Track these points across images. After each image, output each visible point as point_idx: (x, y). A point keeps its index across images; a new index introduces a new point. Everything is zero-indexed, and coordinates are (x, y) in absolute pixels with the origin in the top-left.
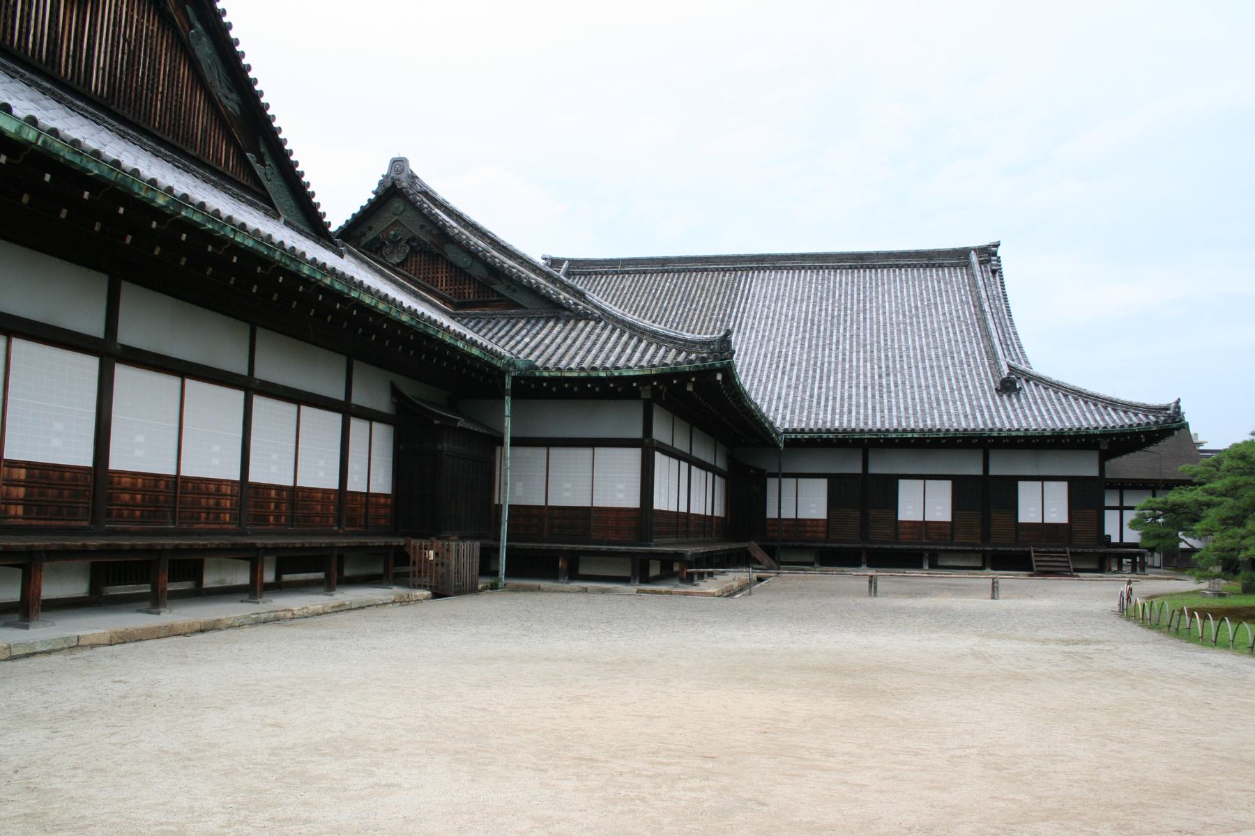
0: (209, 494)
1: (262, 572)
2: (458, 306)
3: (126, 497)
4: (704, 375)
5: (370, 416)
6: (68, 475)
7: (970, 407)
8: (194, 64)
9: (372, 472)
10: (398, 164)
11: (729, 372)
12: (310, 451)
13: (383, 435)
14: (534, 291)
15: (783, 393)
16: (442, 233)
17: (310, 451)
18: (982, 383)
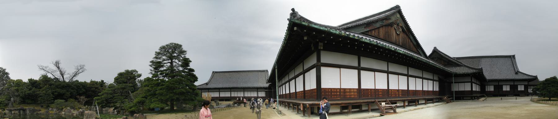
2: (445, 65)
4: (479, 73)
5: (436, 81)
7: (511, 76)
9: (437, 89)
10: (435, 48)
11: (482, 72)
12: (429, 86)
13: (437, 83)
14: (455, 63)
15: (488, 75)
16: (442, 56)
17: (429, 86)
18: (513, 72)
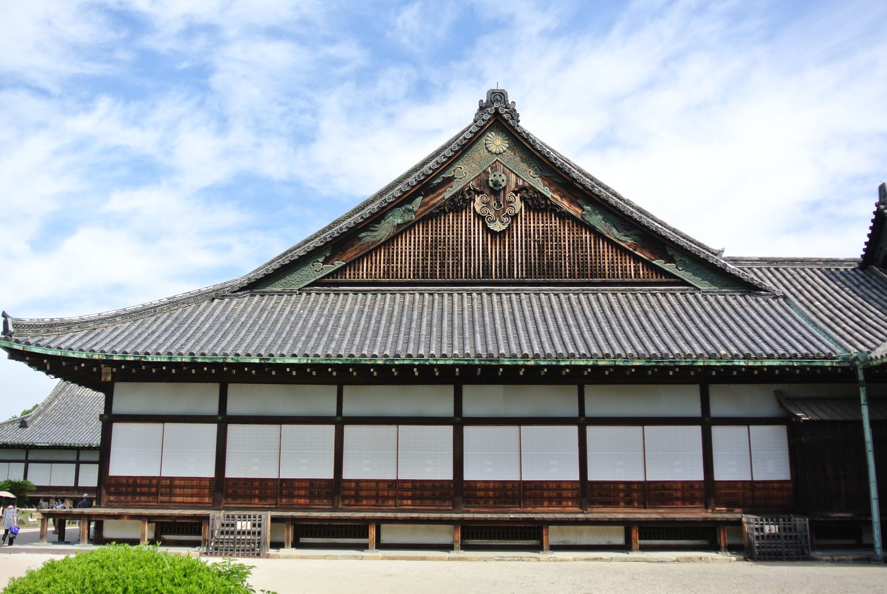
0: (548, 489)
1: (547, 534)
3: (482, 494)
6: (418, 484)
8: (592, 229)
